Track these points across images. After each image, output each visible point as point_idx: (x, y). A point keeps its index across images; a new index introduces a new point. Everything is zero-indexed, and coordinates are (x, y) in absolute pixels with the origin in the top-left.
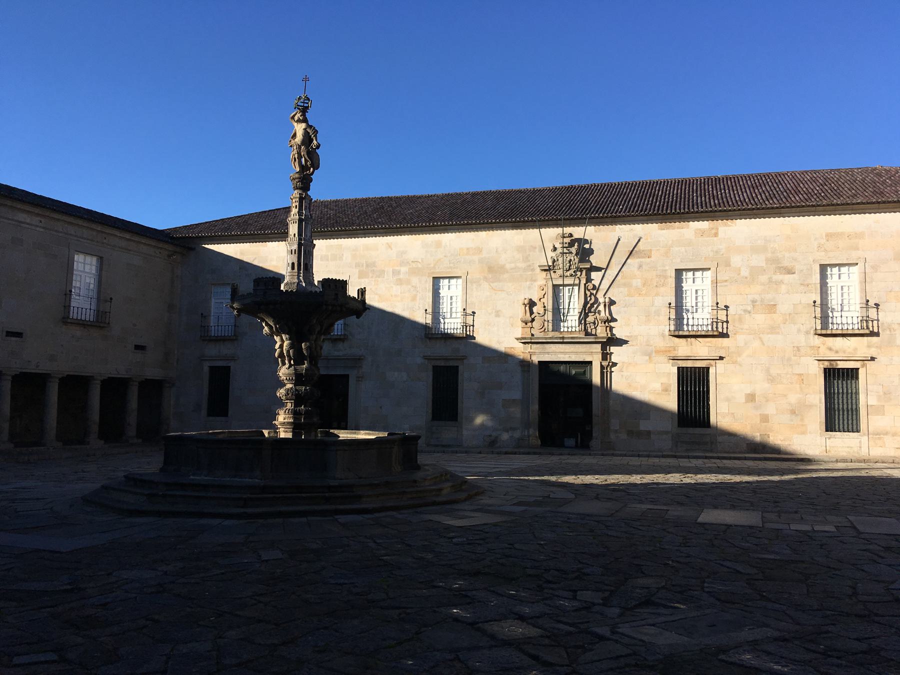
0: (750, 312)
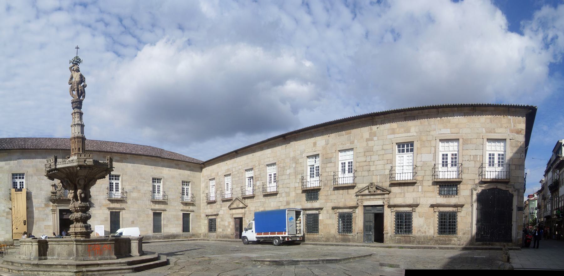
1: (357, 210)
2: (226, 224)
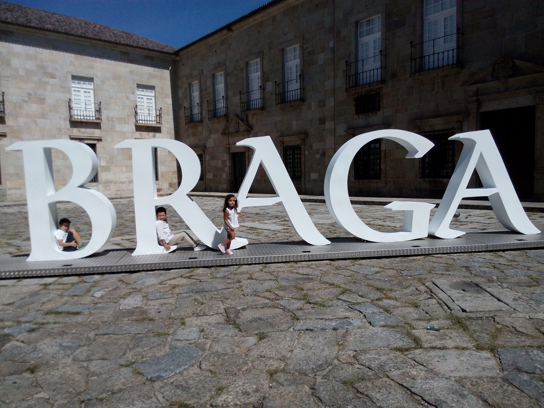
0: (26, 102)
2: (219, 164)
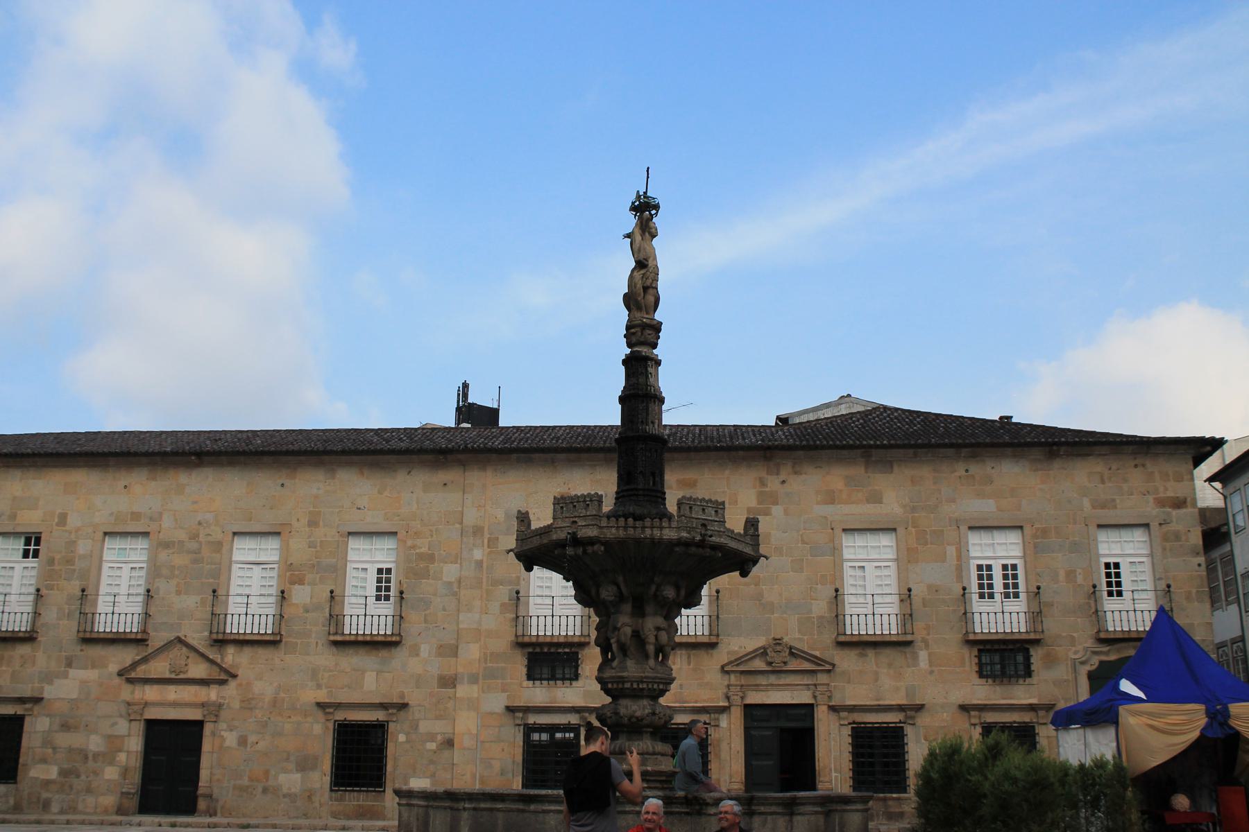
1: (724, 721)
2: (95, 743)
